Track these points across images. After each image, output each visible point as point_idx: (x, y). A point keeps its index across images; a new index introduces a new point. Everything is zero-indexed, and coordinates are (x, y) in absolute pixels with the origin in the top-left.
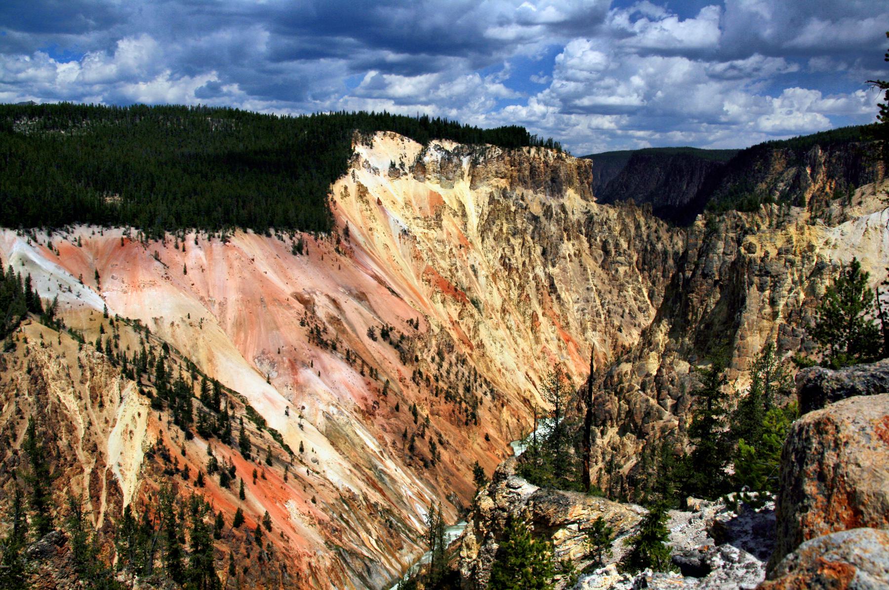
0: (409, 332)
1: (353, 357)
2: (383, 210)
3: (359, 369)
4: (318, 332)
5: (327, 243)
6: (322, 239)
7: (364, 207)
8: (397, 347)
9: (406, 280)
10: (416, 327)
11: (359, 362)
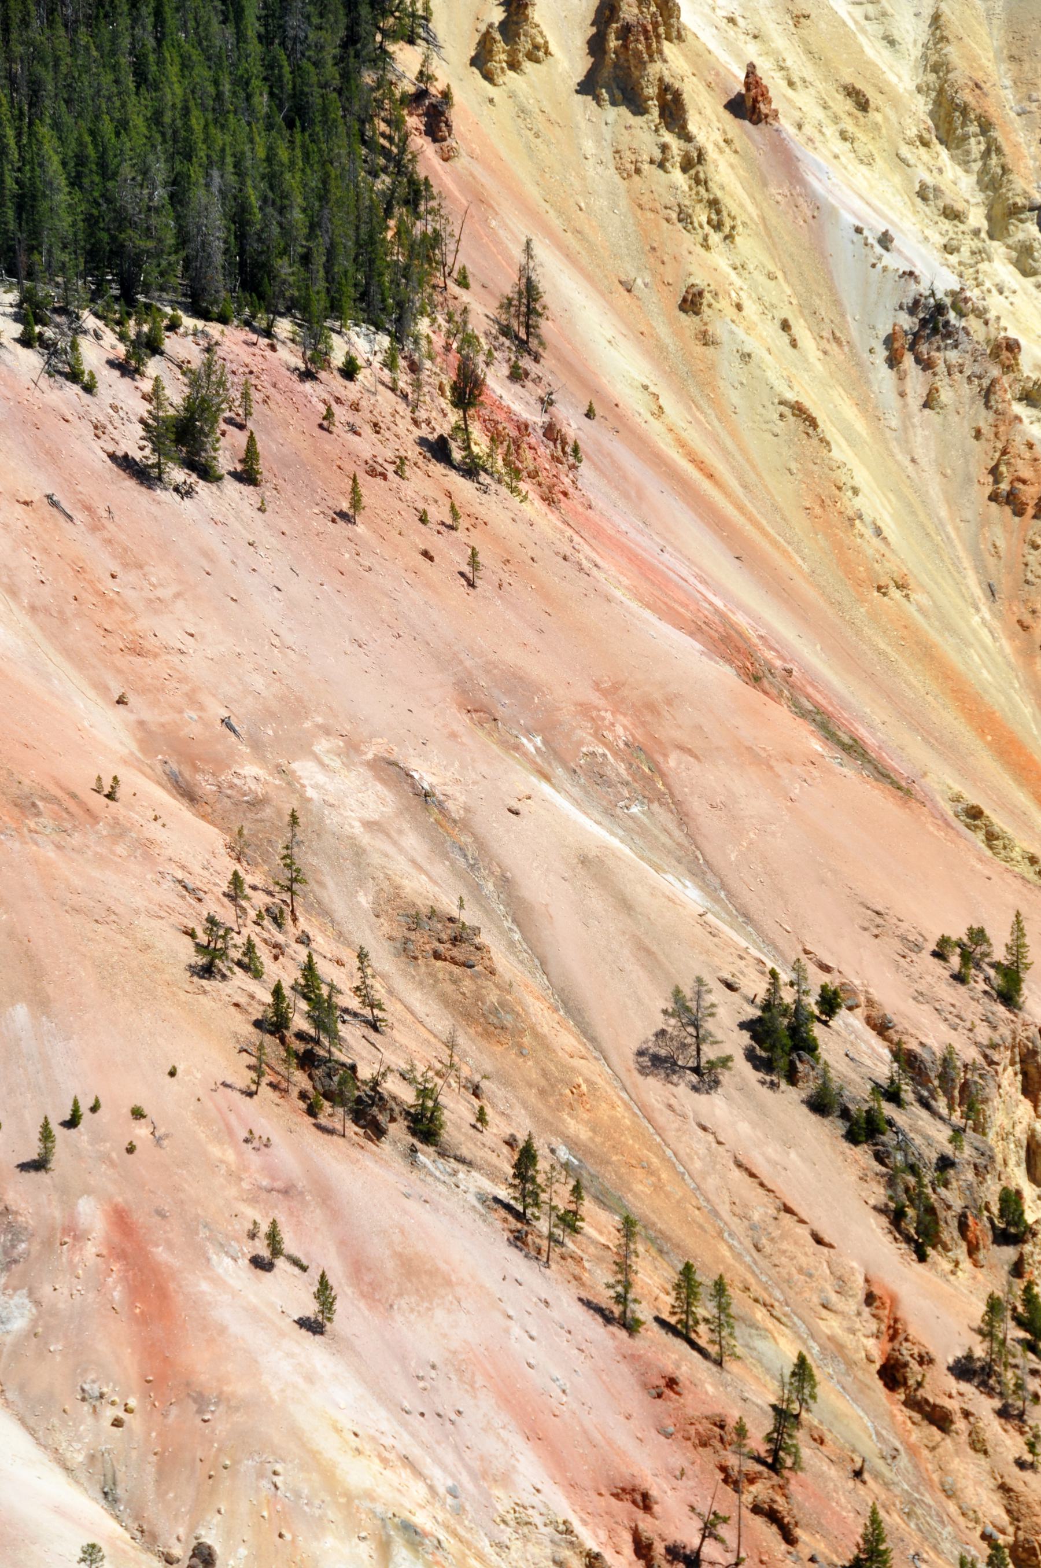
0: (955, 1020)
1: (560, 1197)
2: (786, 163)
3: (601, 1280)
4: (324, 1012)
5: (387, 400)
6: (349, 371)
7: (644, 133)
8: (864, 1129)
9: (927, 654)
10: (1008, 995)
11: (599, 1225)
